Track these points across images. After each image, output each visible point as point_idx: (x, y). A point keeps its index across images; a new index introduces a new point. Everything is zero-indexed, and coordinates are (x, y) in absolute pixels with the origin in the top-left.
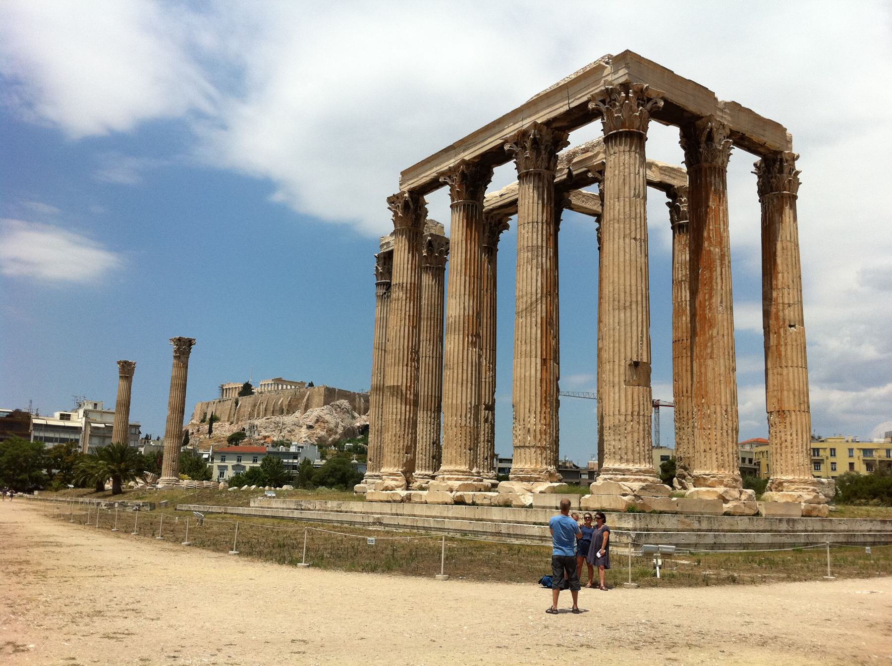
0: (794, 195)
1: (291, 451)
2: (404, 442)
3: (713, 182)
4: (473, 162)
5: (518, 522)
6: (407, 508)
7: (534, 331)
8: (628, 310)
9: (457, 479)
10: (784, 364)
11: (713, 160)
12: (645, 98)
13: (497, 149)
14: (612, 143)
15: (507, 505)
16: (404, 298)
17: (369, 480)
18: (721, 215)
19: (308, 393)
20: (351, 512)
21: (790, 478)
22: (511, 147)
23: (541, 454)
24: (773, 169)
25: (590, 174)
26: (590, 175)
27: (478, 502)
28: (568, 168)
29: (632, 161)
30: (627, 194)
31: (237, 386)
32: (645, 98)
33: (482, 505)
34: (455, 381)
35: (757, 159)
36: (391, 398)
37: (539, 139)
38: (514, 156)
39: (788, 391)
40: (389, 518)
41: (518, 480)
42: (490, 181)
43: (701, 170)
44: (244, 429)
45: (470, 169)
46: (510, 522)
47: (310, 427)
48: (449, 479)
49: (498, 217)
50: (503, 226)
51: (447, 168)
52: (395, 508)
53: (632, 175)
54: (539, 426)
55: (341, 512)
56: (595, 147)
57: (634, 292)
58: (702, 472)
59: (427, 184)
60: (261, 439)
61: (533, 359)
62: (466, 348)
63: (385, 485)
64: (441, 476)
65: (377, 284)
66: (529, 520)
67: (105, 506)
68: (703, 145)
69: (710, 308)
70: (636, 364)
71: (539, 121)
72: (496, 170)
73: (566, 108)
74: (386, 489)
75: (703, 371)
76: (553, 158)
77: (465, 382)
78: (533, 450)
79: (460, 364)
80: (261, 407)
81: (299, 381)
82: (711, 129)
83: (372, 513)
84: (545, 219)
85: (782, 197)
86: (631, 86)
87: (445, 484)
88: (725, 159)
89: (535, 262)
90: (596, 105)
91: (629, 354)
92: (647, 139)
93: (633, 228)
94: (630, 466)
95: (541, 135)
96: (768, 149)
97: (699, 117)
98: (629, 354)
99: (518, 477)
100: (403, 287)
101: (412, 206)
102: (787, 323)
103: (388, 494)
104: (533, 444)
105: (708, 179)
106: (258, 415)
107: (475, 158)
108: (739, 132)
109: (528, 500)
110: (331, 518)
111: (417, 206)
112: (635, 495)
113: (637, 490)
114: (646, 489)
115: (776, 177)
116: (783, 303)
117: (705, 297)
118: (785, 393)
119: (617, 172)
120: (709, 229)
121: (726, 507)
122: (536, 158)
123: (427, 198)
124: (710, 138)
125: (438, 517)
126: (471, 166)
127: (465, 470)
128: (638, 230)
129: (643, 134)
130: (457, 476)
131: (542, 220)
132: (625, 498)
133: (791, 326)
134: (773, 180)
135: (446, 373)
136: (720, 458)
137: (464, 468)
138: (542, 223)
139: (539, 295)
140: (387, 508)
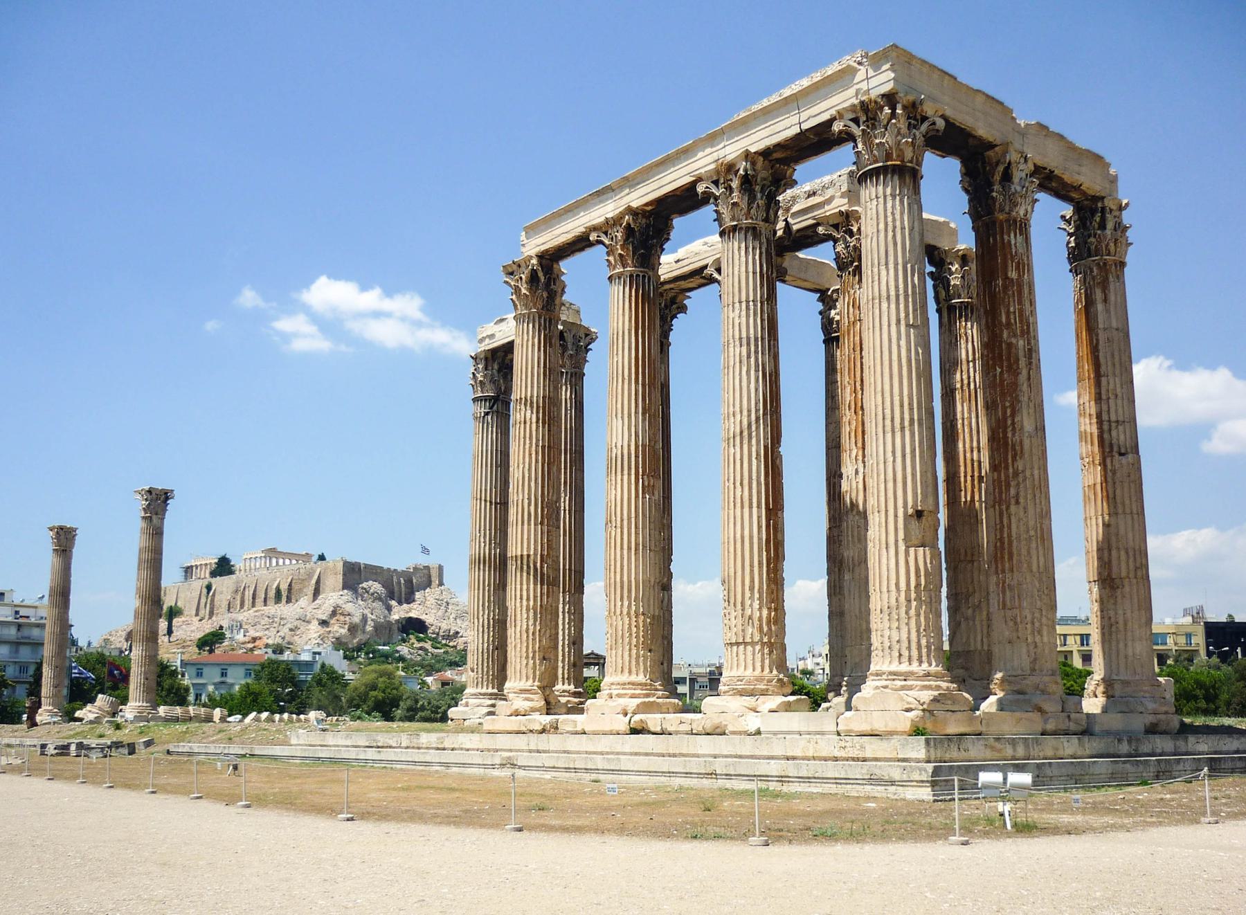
0: (1121, 262)
1: (302, 659)
3: (1013, 242)
4: (642, 210)
5: (741, 757)
6: (552, 742)
9: (633, 696)
11: (1011, 210)
12: (919, 117)
13: (682, 191)
14: (871, 181)
15: (718, 731)
16: (534, 420)
17: (471, 701)
18: (1026, 291)
20: (462, 749)
22: (707, 187)
23: (771, 652)
24: (1091, 223)
26: (821, 230)
27: (670, 729)
28: (784, 220)
31: (208, 562)
32: (919, 117)
33: (677, 733)
34: (625, 546)
36: (518, 574)
37: (753, 176)
38: (712, 200)
39: (1118, 549)
40: (528, 756)
41: (734, 694)
42: (668, 239)
43: (994, 223)
44: (221, 628)
47: (324, 623)
48: (619, 696)
49: (671, 295)
50: (678, 308)
51: (602, 219)
52: (535, 741)
54: (765, 612)
55: (444, 749)
56: (827, 189)
59: (568, 244)
60: (249, 642)
61: (755, 510)
62: (641, 496)
63: (515, 707)
64: (608, 692)
65: (475, 400)
66: (757, 753)
67: (55, 749)
69: (1014, 429)
71: (753, 149)
73: (796, 130)
74: (517, 713)
75: (1005, 521)
76: (772, 204)
80: (247, 593)
81: (304, 553)
82: (1010, 163)
83: (497, 751)
86: (898, 99)
87: (614, 704)
88: (1029, 210)
90: (845, 126)
92: (922, 177)
95: (754, 170)
96: (1084, 193)
97: (991, 146)
99: (734, 689)
100: (532, 403)
101: (542, 279)
103: (520, 721)
105: (1006, 237)
107: (647, 204)
108: (1045, 169)
110: (428, 759)
111: (550, 278)
113: (927, 702)
114: (939, 701)
116: (1109, 421)
117: (1006, 412)
118: (1114, 553)
119: (882, 226)
120: (1008, 313)
122: (749, 204)
123: (565, 266)
124: (1007, 177)
125: (608, 753)
126: (640, 215)
127: (644, 681)
129: (918, 170)
130: (633, 692)
133: (1121, 454)
134: (1092, 239)
137: (641, 678)
138: (762, 303)
140: (520, 742)
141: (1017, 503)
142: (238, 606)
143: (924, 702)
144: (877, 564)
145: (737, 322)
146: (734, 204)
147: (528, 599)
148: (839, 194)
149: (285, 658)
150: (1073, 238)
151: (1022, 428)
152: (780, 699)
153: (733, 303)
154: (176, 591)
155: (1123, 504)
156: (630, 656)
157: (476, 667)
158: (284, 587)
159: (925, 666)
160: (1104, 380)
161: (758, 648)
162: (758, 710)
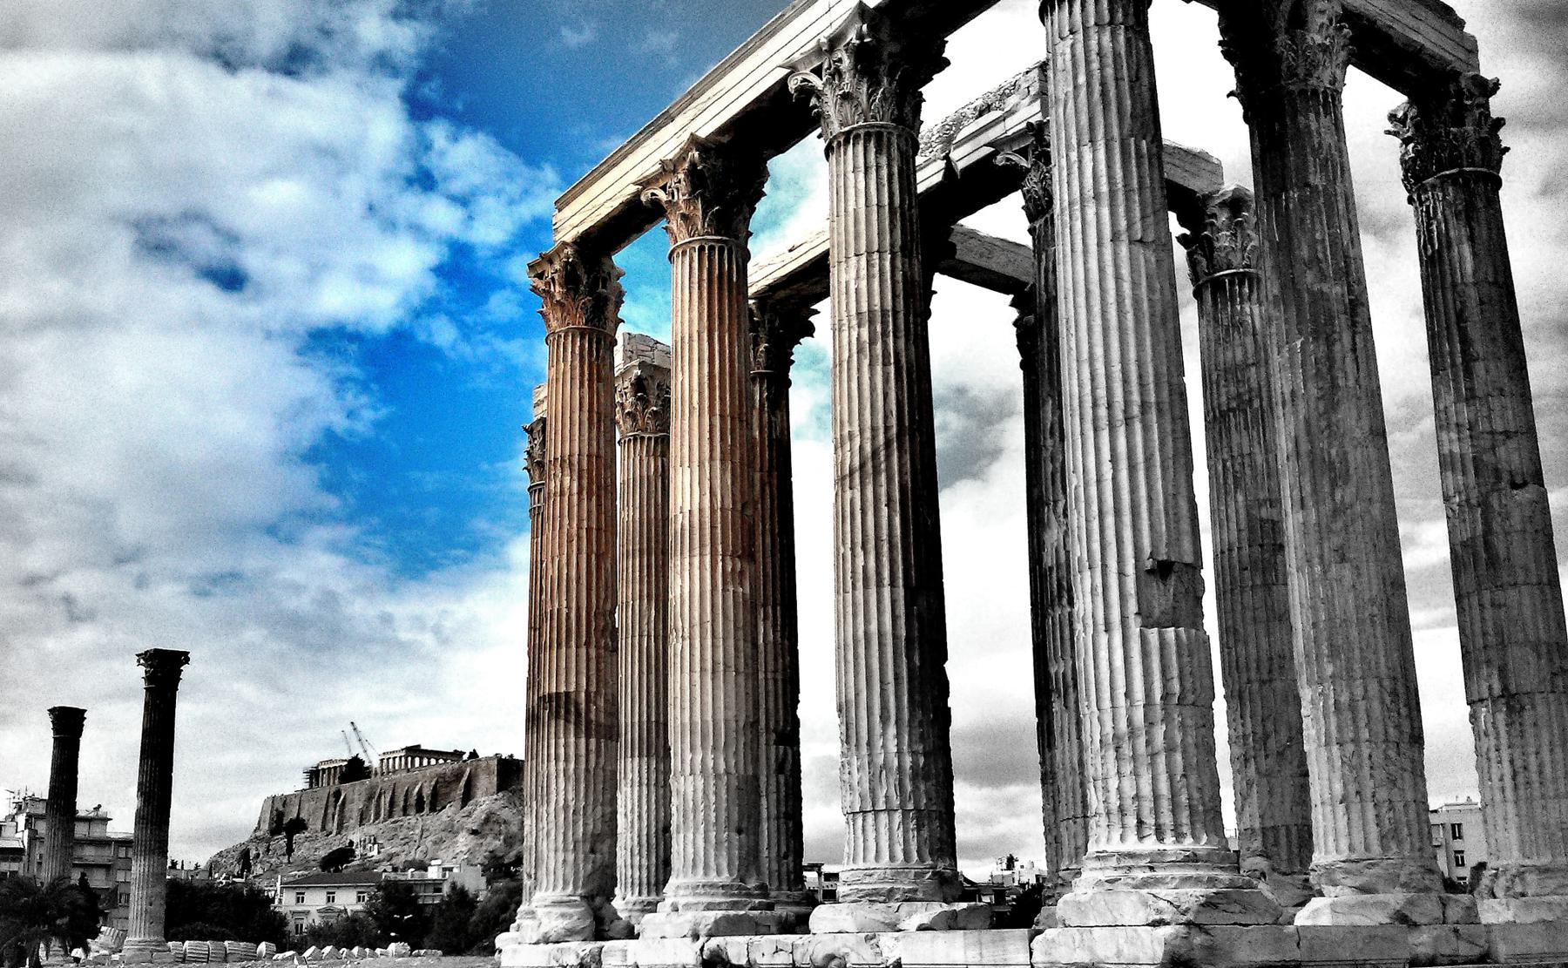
2: (585, 824)
9: (709, 907)
19: (468, 770)
23: (919, 828)
25: (999, 157)
26: (1000, 160)
28: (945, 158)
45: (712, 161)
47: (474, 832)
84: (899, 242)
85: (1466, 182)
89: (879, 347)
106: (377, 815)
113: (1195, 907)
115: (1447, 134)
122: (869, 96)
127: (728, 882)
130: (710, 899)
131: (892, 246)
135: (677, 646)
136: (1387, 816)
142: (372, 818)
143: (1187, 910)
144: (1091, 662)
145: (853, 287)
146: (846, 97)
147: (566, 760)
148: (1028, 100)
149: (409, 878)
150: (1412, 145)
152: (938, 908)
153: (847, 258)
154: (297, 801)
156: (706, 840)
157: (533, 872)
158: (427, 792)
159: (1188, 843)
161: (898, 817)
162: (900, 927)
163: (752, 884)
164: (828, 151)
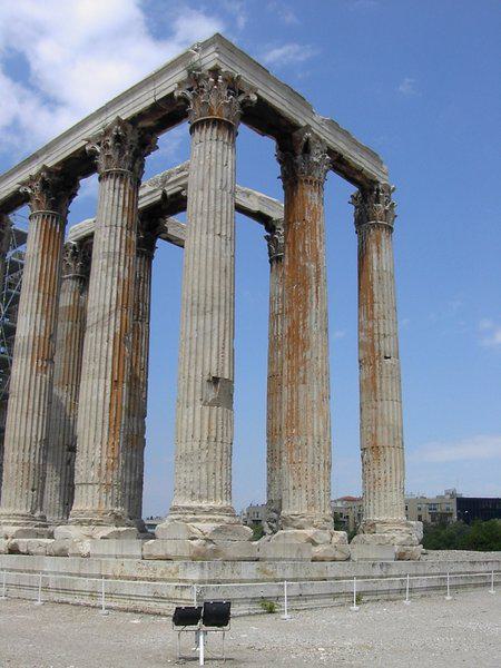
4: (57, 172)
5: (71, 574)
7: (105, 347)
8: (209, 315)
9: (15, 524)
10: (378, 398)
15: (63, 553)
21: (383, 518)
29: (220, 151)
30: (213, 186)
33: (37, 554)
34: (19, 411)
35: (354, 190)
42: (75, 195)
46: (62, 574)
53: (219, 166)
57: (216, 295)
58: (290, 512)
61: (102, 381)
68: (299, 157)
70: (215, 380)
72: (82, 182)
73: (152, 101)
77: (30, 412)
78: (97, 487)
79: (27, 393)
82: (308, 139)
84: (125, 223)
89: (110, 270)
91: (207, 368)
93: (218, 223)
94: (204, 504)
97: (296, 127)
98: (207, 368)
102: (383, 354)
104: (97, 480)
107: (56, 165)
109: (86, 547)
112: (206, 539)
118: (379, 429)
119: (202, 162)
121: (318, 551)
124: (307, 149)
128: (224, 227)
132: (194, 542)
133: (386, 358)
136: (311, 496)
137: (23, 511)
139: (113, 308)
141: (304, 383)
151: (311, 327)
155: (387, 393)
160: (376, 306)
161: (97, 487)
163: (37, 515)
164: (100, 179)
